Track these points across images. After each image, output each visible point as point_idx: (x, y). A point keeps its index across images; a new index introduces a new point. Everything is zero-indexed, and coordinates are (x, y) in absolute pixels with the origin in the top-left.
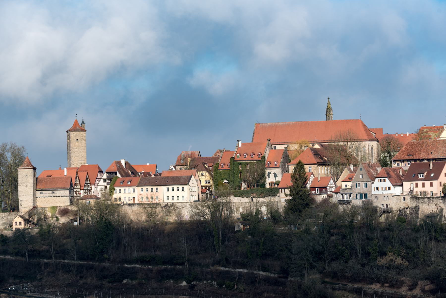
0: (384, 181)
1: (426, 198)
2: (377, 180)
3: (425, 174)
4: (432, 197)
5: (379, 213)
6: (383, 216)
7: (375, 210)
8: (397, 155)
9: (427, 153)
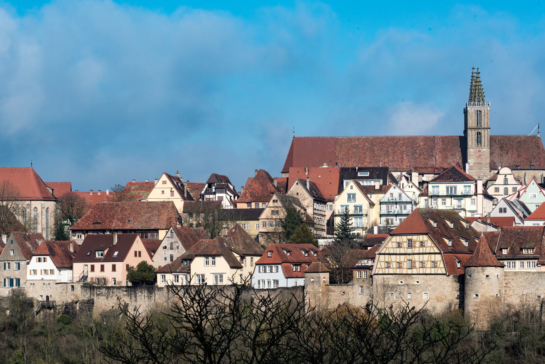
0: (44, 261)
1: (104, 287)
2: (34, 258)
3: (106, 251)
4: (113, 287)
5: (36, 309)
6: (42, 313)
7: (30, 303)
8: (80, 223)
9: (122, 220)
